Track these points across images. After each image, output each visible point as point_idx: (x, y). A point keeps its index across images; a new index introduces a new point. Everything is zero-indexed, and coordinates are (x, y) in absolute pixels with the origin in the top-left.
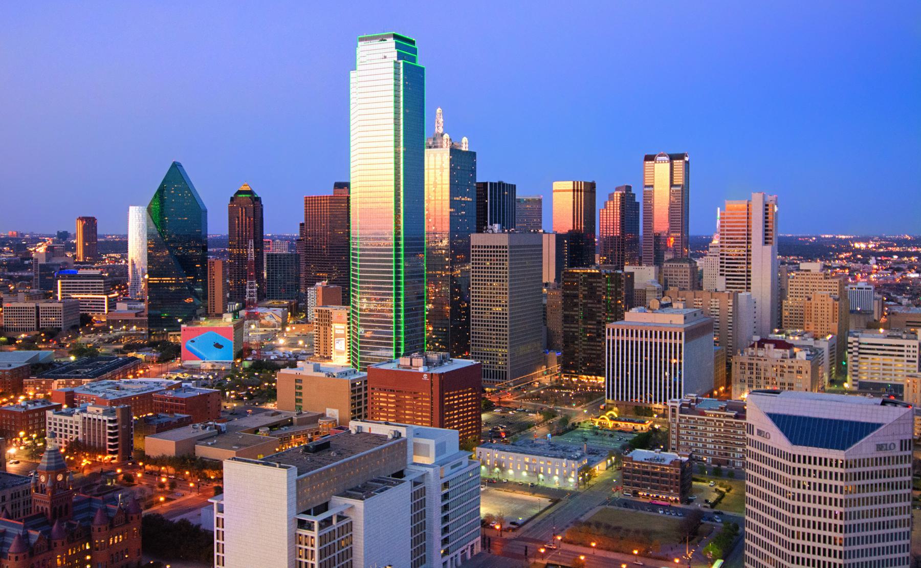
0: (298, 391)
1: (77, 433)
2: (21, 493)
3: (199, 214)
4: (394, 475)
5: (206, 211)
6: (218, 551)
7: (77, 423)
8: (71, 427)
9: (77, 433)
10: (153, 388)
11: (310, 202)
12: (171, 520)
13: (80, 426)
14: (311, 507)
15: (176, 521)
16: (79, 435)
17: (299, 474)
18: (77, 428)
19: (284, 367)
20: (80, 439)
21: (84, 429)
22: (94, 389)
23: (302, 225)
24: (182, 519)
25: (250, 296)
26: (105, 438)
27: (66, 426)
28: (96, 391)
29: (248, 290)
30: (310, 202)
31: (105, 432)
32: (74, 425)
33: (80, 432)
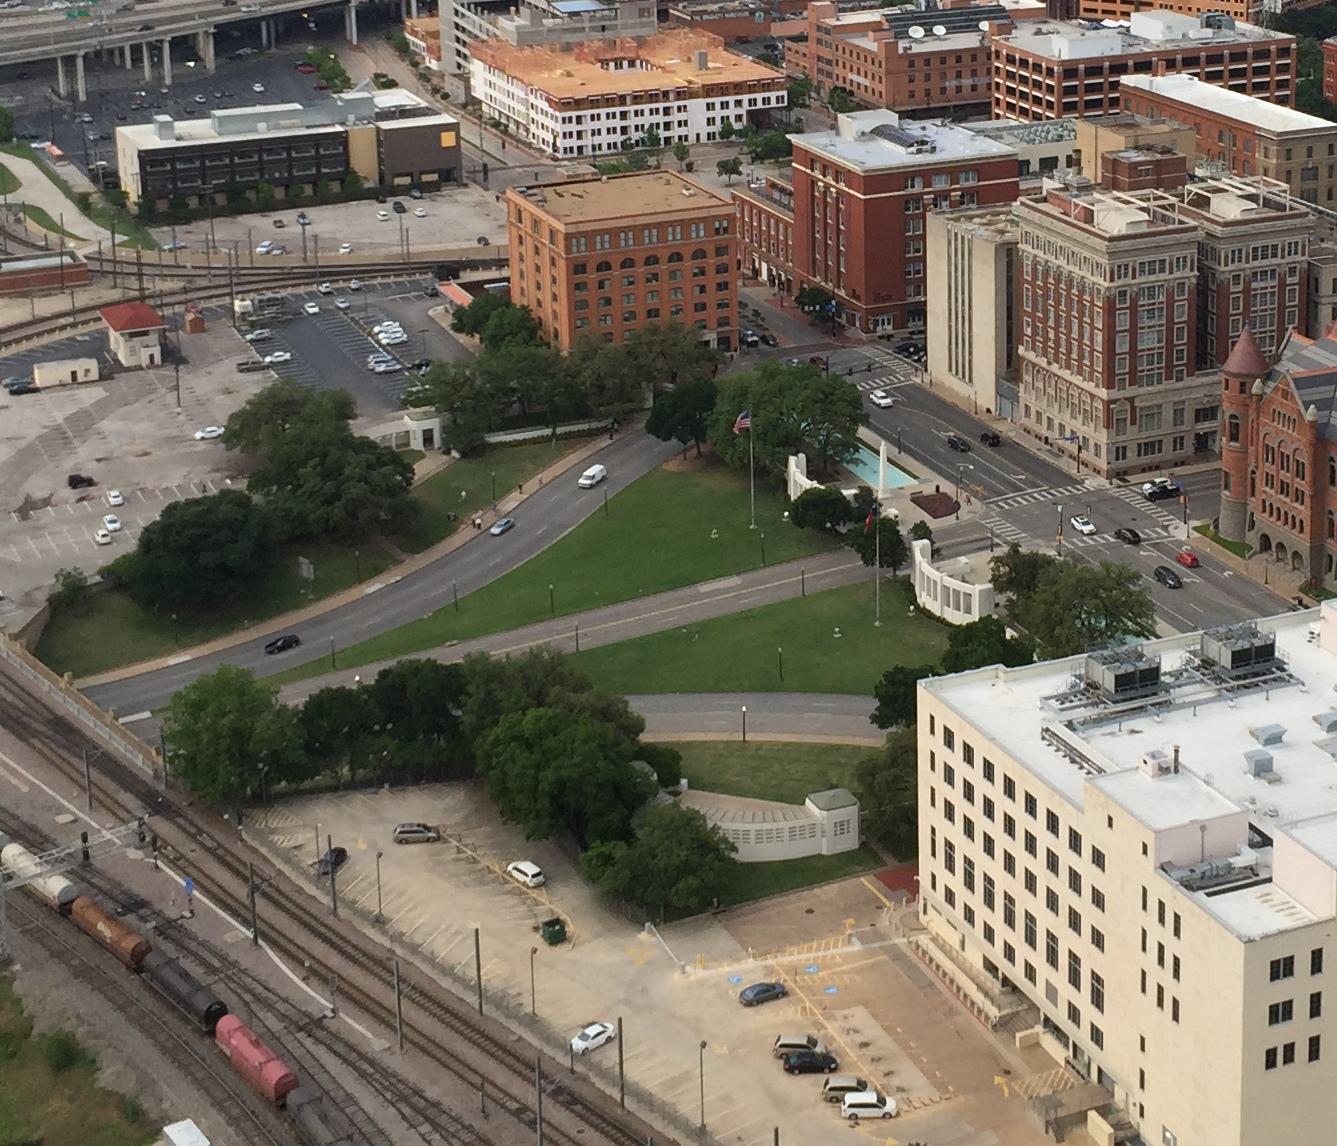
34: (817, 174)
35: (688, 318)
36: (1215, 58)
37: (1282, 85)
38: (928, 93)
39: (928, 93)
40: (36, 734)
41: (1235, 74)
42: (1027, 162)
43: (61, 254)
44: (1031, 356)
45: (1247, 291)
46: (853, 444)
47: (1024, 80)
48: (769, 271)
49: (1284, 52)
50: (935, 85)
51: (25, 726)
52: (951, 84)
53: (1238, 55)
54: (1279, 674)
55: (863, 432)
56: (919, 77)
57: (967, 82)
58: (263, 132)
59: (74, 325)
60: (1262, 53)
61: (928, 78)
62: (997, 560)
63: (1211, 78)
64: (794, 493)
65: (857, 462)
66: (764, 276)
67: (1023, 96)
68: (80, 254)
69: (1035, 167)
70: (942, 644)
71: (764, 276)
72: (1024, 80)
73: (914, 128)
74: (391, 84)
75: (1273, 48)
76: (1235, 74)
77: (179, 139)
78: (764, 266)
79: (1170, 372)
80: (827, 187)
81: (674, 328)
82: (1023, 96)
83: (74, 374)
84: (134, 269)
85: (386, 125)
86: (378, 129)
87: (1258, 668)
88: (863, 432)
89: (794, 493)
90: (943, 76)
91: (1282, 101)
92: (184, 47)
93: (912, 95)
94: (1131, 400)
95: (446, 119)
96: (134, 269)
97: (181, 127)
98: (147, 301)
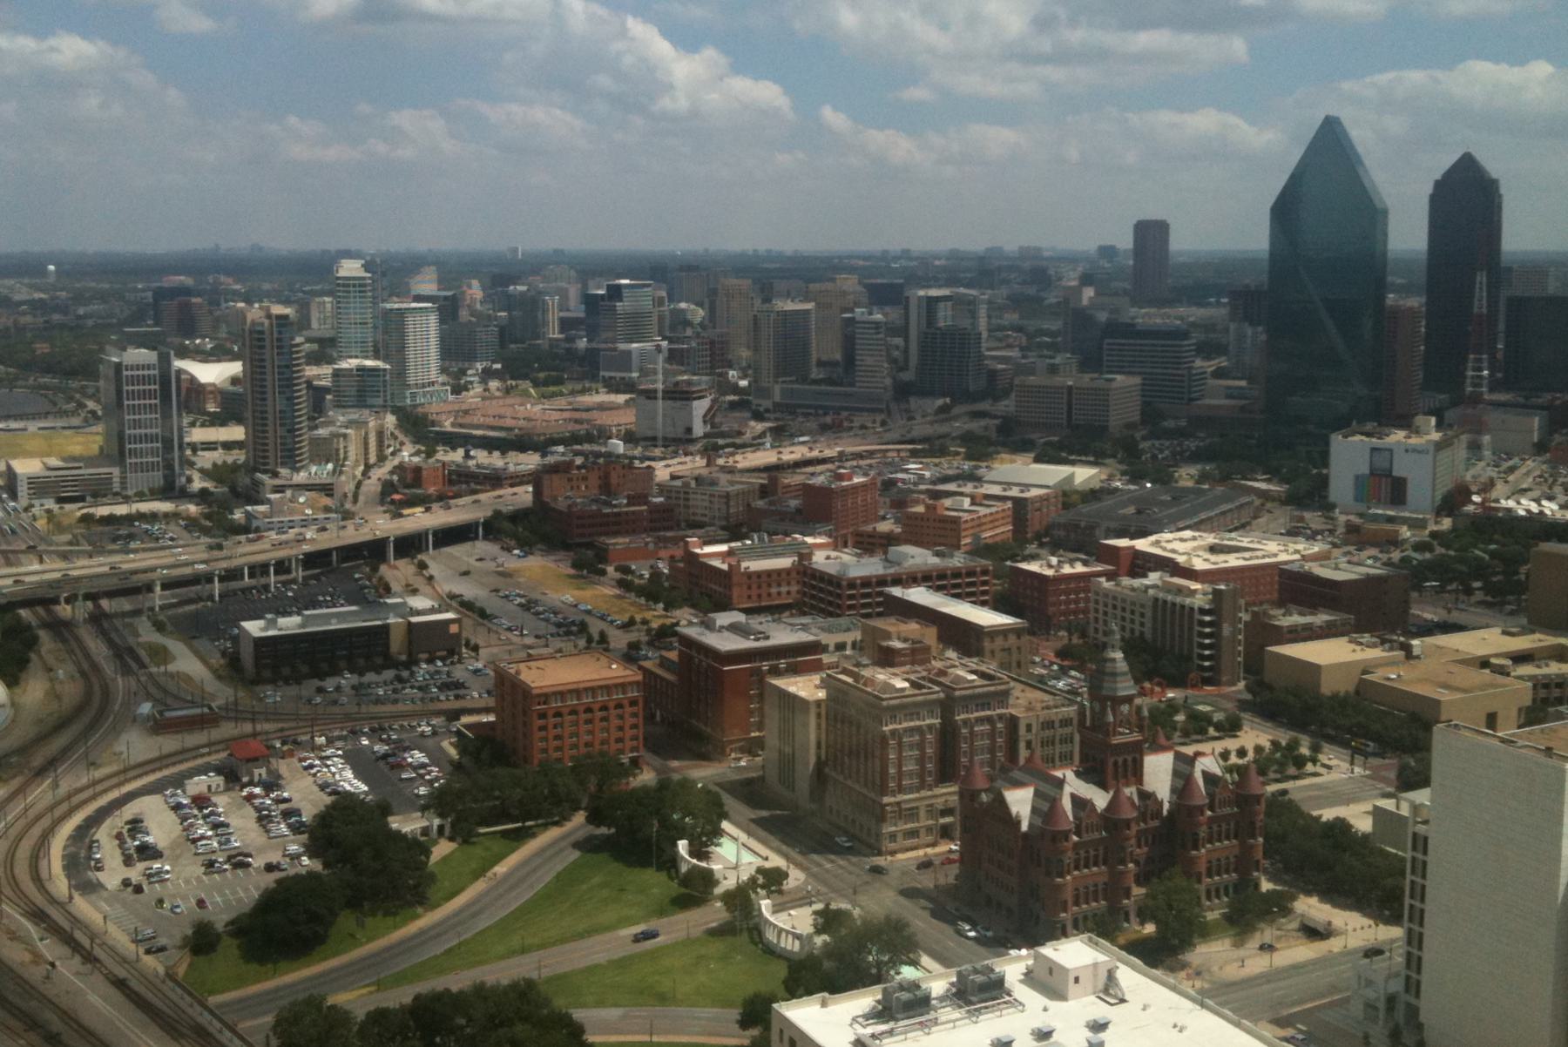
1: (1142, 624)
2: (1057, 724)
3: (1370, 215)
6: (1412, 897)
7: (1142, 606)
8: (1133, 612)
9: (1142, 624)
10: (1275, 555)
13: (1149, 613)
15: (1324, 819)
16: (1145, 630)
18: (1142, 615)
20: (1148, 635)
21: (1155, 619)
22: (1169, 546)
24: (1337, 819)
25: (1474, 385)
26: (1190, 640)
27: (1124, 610)
28: (1174, 551)
29: (1470, 373)
31: (1191, 629)
32: (1138, 609)
33: (1149, 625)
34: (694, 653)
35: (614, 746)
36: (942, 576)
37: (984, 593)
38: (759, 596)
39: (759, 596)
40: (183, 1036)
41: (955, 586)
42: (827, 646)
43: (203, 706)
44: (833, 774)
45: (972, 733)
46: (719, 832)
47: (821, 590)
48: (662, 715)
49: (985, 572)
50: (764, 591)
51: (176, 1030)
52: (774, 590)
53: (957, 574)
54: (1007, 998)
55: (725, 825)
56: (754, 586)
57: (784, 589)
58: (334, 626)
59: (209, 754)
60: (971, 573)
61: (759, 587)
62: (816, 913)
63: (939, 589)
64: (684, 868)
65: (718, 845)
66: (658, 718)
67: (822, 600)
68: (213, 705)
69: (831, 648)
70: (781, 971)
71: (658, 718)
72: (821, 590)
73: (756, 622)
74: (414, 592)
75: (978, 569)
76: (955, 586)
77: (281, 629)
78: (658, 713)
79: (922, 786)
80: (700, 661)
81: (602, 754)
82: (822, 600)
83: (209, 787)
84: (250, 716)
85: (414, 619)
86: (410, 623)
87: (995, 993)
88: (725, 825)
89: (684, 868)
90: (769, 585)
91: (983, 604)
92: (282, 567)
93: (749, 597)
94: (898, 804)
95: (450, 615)
96: (250, 716)
97: (282, 621)
98: (259, 738)
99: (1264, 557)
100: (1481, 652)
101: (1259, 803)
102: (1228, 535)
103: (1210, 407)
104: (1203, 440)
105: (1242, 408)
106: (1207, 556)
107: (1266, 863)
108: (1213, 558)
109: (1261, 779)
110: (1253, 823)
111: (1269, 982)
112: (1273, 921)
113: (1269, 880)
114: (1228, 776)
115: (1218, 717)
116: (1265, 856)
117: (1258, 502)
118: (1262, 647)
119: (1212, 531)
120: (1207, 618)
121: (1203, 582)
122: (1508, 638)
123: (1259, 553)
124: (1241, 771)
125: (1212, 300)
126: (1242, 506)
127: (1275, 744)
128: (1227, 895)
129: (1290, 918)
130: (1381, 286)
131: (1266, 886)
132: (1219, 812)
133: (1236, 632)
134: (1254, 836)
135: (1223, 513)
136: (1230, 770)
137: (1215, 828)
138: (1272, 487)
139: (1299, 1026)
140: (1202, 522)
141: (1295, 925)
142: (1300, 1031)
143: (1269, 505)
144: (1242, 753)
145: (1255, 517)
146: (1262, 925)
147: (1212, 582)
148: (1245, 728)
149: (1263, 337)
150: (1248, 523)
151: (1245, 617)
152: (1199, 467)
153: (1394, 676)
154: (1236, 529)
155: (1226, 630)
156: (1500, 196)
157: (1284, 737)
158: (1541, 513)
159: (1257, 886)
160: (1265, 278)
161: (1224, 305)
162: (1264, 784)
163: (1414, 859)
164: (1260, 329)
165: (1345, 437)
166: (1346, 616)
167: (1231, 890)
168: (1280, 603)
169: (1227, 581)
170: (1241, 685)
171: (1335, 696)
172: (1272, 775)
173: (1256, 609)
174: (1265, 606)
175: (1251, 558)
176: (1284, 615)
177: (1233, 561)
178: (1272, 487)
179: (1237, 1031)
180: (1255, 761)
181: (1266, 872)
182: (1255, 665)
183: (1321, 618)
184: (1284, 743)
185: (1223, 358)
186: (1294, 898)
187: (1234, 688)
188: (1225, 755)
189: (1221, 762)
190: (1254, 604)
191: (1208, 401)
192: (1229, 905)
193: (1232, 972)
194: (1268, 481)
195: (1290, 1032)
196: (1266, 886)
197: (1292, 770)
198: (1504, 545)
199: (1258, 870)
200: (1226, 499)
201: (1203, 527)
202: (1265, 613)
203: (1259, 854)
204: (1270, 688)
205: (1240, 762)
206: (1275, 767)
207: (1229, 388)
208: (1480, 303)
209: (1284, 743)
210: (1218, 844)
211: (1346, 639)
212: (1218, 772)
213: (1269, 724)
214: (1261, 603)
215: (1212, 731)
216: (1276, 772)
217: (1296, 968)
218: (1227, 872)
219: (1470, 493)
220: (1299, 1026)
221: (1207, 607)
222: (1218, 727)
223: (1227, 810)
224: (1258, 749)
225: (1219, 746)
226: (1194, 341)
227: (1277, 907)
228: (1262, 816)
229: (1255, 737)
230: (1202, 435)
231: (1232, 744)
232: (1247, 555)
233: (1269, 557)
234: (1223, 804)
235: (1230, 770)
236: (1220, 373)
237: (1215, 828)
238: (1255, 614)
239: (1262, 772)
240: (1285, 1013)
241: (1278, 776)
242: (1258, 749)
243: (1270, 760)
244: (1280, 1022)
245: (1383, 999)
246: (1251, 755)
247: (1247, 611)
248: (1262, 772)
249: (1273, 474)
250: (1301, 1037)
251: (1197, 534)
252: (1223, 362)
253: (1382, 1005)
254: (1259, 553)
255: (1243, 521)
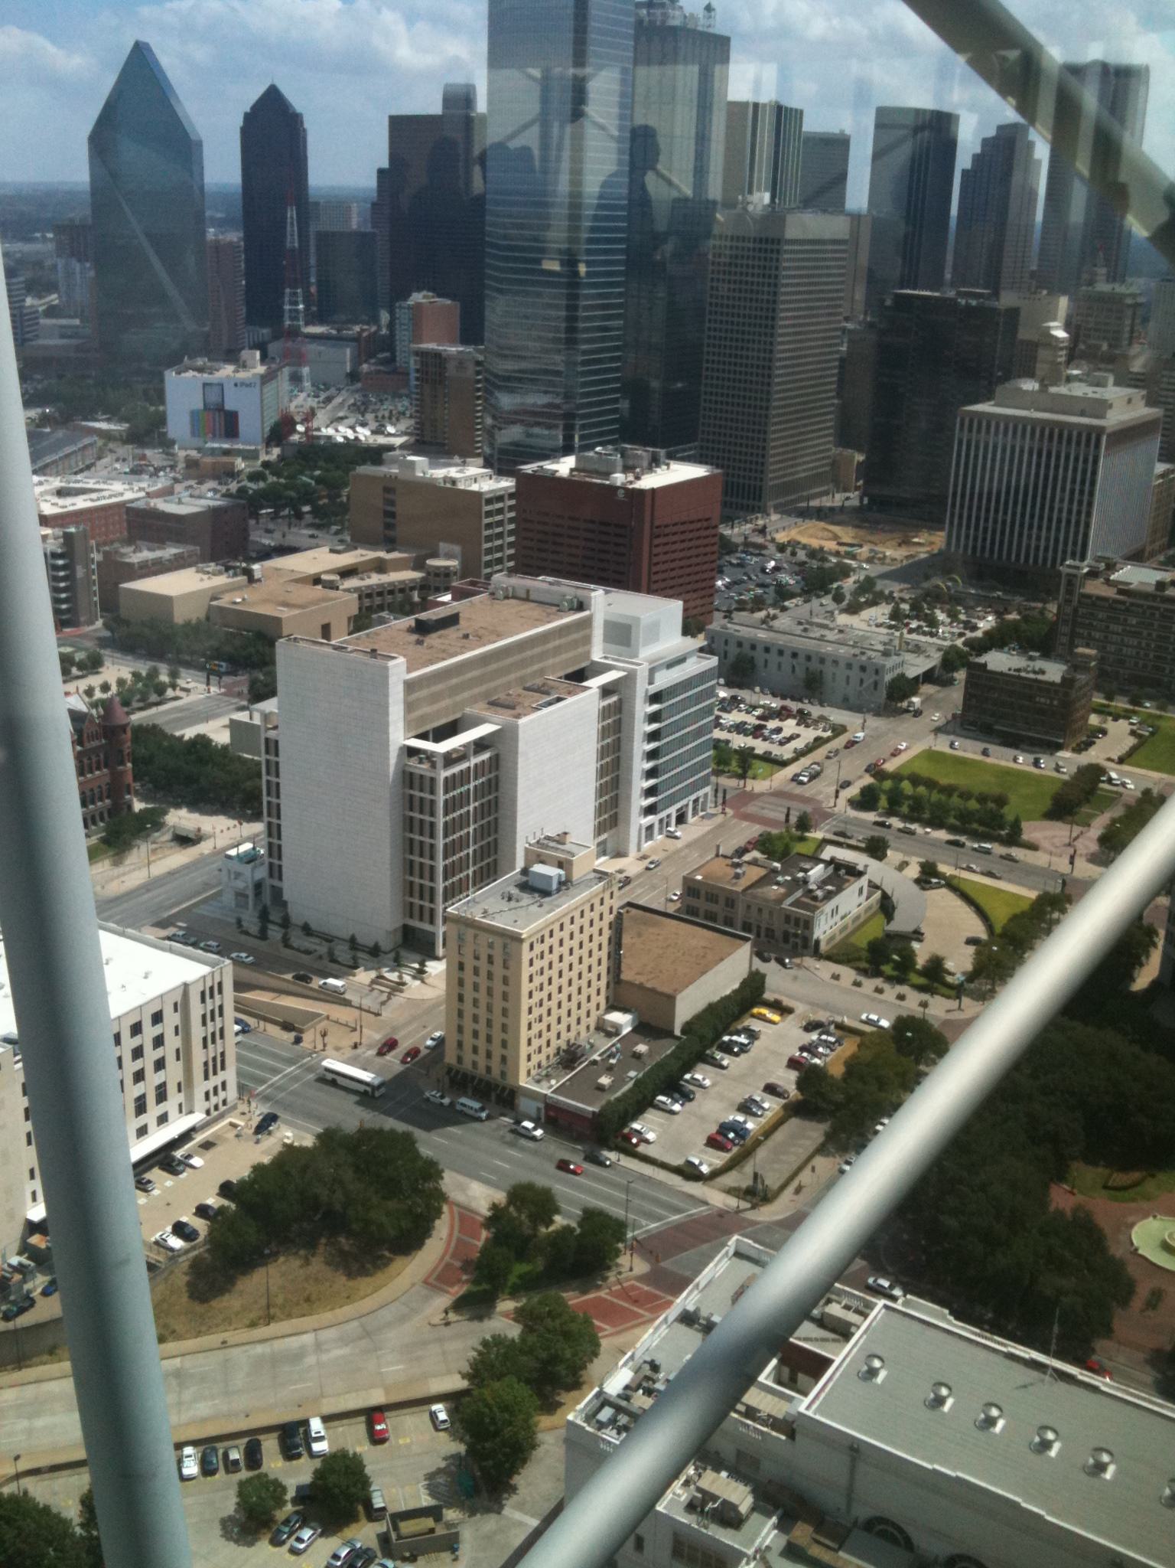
0: (389, 508)
4: (568, 677)
5: (199, 144)
10: (122, 494)
11: (402, 127)
12: (178, 734)
14: (429, 727)
17: (409, 671)
19: (364, 462)
23: (381, 172)
25: (292, 319)
29: (287, 307)
30: (402, 127)
99: (110, 497)
100: (313, 570)
101: (125, 732)
102: (74, 478)
103: (46, 348)
104: (40, 381)
105: (78, 349)
106: (55, 500)
107: (137, 786)
108: (61, 501)
109: (126, 709)
110: (121, 751)
111: (148, 891)
112: (148, 836)
113: (141, 801)
114: (94, 712)
115: (79, 656)
116: (135, 779)
117: (100, 443)
118: (116, 584)
119: (57, 474)
120: (60, 562)
121: (53, 527)
122: (335, 556)
123: (106, 494)
124: (106, 704)
125: (38, 235)
126: (85, 447)
127: (136, 675)
128: (102, 819)
129: (164, 830)
130: (200, 220)
131: (138, 806)
132: (89, 745)
133: (88, 574)
134: (122, 763)
135: (67, 456)
136: (94, 705)
137: (86, 761)
138: (113, 427)
139: (180, 924)
140: (46, 466)
141: (168, 836)
142: (180, 928)
143: (111, 445)
144: (105, 687)
145: (99, 458)
146: (138, 842)
147: (62, 526)
148: (108, 663)
149: (92, 273)
150: (93, 464)
151: (97, 557)
152: (39, 410)
153: (239, 600)
154: (81, 471)
155: (80, 572)
156: (304, 130)
157: (143, 668)
158: (357, 438)
159: (130, 807)
160: (88, 212)
161: (51, 240)
162: (128, 714)
163: (268, 761)
164: (88, 265)
165: (179, 373)
166: (191, 548)
167: (106, 815)
168: (130, 541)
169: (77, 524)
170: (99, 623)
171: (188, 624)
172: (135, 705)
173: (107, 548)
174: (116, 545)
175: (98, 499)
176: (134, 552)
177: (81, 503)
178: (113, 427)
179: (123, 939)
180: (119, 694)
181: (137, 793)
182: (110, 603)
183: (170, 552)
184: (144, 673)
185: (54, 296)
186: (165, 813)
187: (91, 628)
188: (89, 692)
189: (87, 699)
190: (105, 544)
191: (41, 342)
192: (105, 830)
193: (115, 888)
194: (108, 420)
195: (171, 931)
196: (138, 806)
197: (154, 698)
198: (327, 470)
199: (129, 793)
200: (72, 441)
201: (48, 471)
202: (116, 552)
203: (129, 778)
204: (127, 623)
205: (105, 696)
206: (138, 697)
207: (62, 327)
208: (292, 240)
209: (144, 673)
210: (89, 776)
211: (193, 569)
212: (84, 708)
213: (129, 658)
214: (112, 542)
215: (74, 671)
216: (139, 701)
217: (172, 874)
218: (101, 799)
219: (295, 423)
220: (180, 924)
221: (59, 551)
222: (81, 666)
223: (95, 744)
224: (121, 682)
225: (83, 684)
226: (21, 279)
227: (147, 824)
228: (129, 744)
229: (117, 671)
230: (39, 377)
231: (95, 681)
232: (94, 496)
233: (115, 496)
234: (92, 737)
235: (94, 705)
236: (51, 312)
237: (86, 761)
238: (106, 554)
239: (126, 703)
240: (166, 915)
241: (141, 704)
242: (121, 682)
243: (132, 691)
244: (162, 924)
245: (251, 886)
246: (114, 689)
247: (98, 551)
248: (126, 703)
249: (113, 414)
250: (181, 933)
251: (42, 478)
252: (53, 298)
253: (250, 893)
254: (106, 494)
255: (88, 462)
